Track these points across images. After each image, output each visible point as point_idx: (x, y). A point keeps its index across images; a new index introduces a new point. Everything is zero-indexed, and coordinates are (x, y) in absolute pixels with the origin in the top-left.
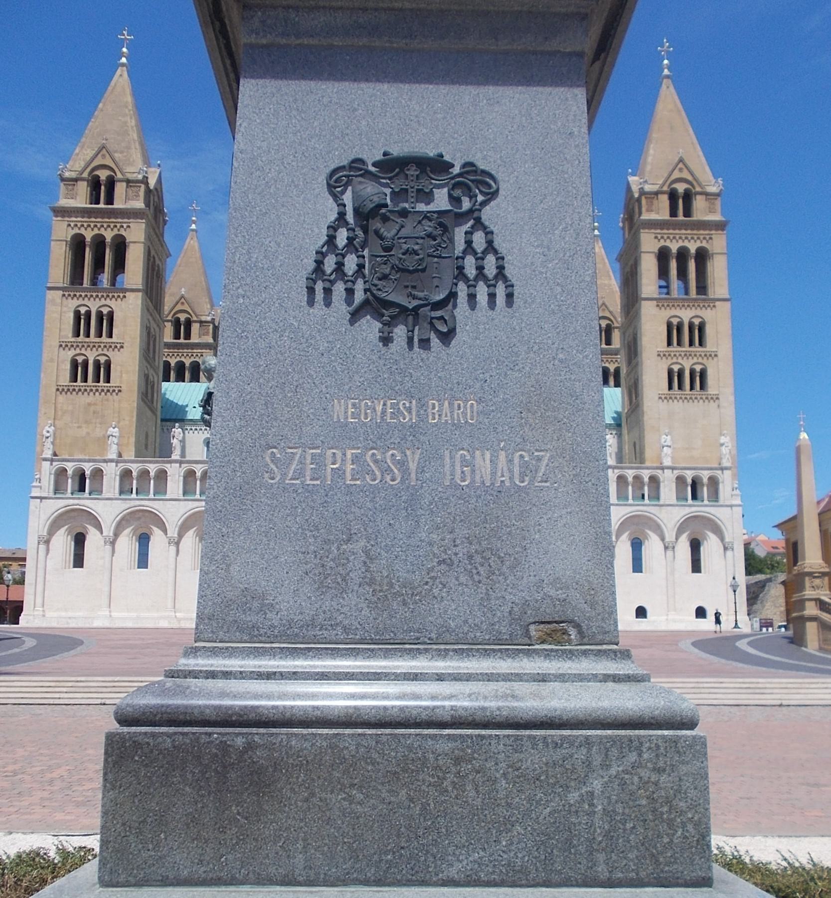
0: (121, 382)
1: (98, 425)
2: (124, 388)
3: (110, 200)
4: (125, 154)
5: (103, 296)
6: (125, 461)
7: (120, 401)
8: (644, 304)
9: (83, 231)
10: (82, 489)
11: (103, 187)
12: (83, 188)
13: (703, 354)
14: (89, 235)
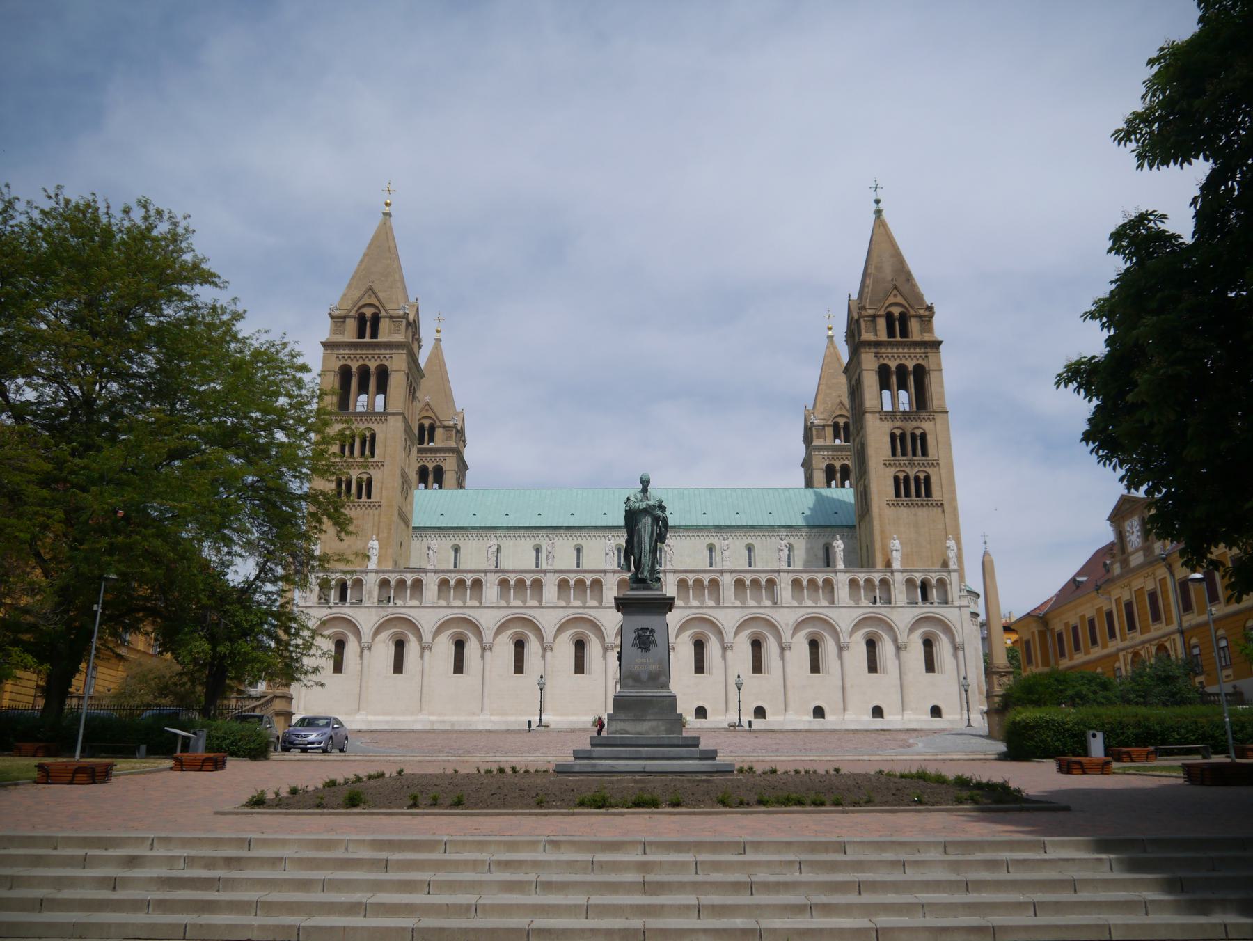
0: (381, 498)
2: (384, 503)
3: (374, 334)
5: (366, 420)
6: (383, 572)
7: (380, 515)
8: (868, 417)
9: (349, 362)
10: (343, 598)
11: (368, 323)
12: (352, 325)
13: (925, 463)
14: (354, 366)
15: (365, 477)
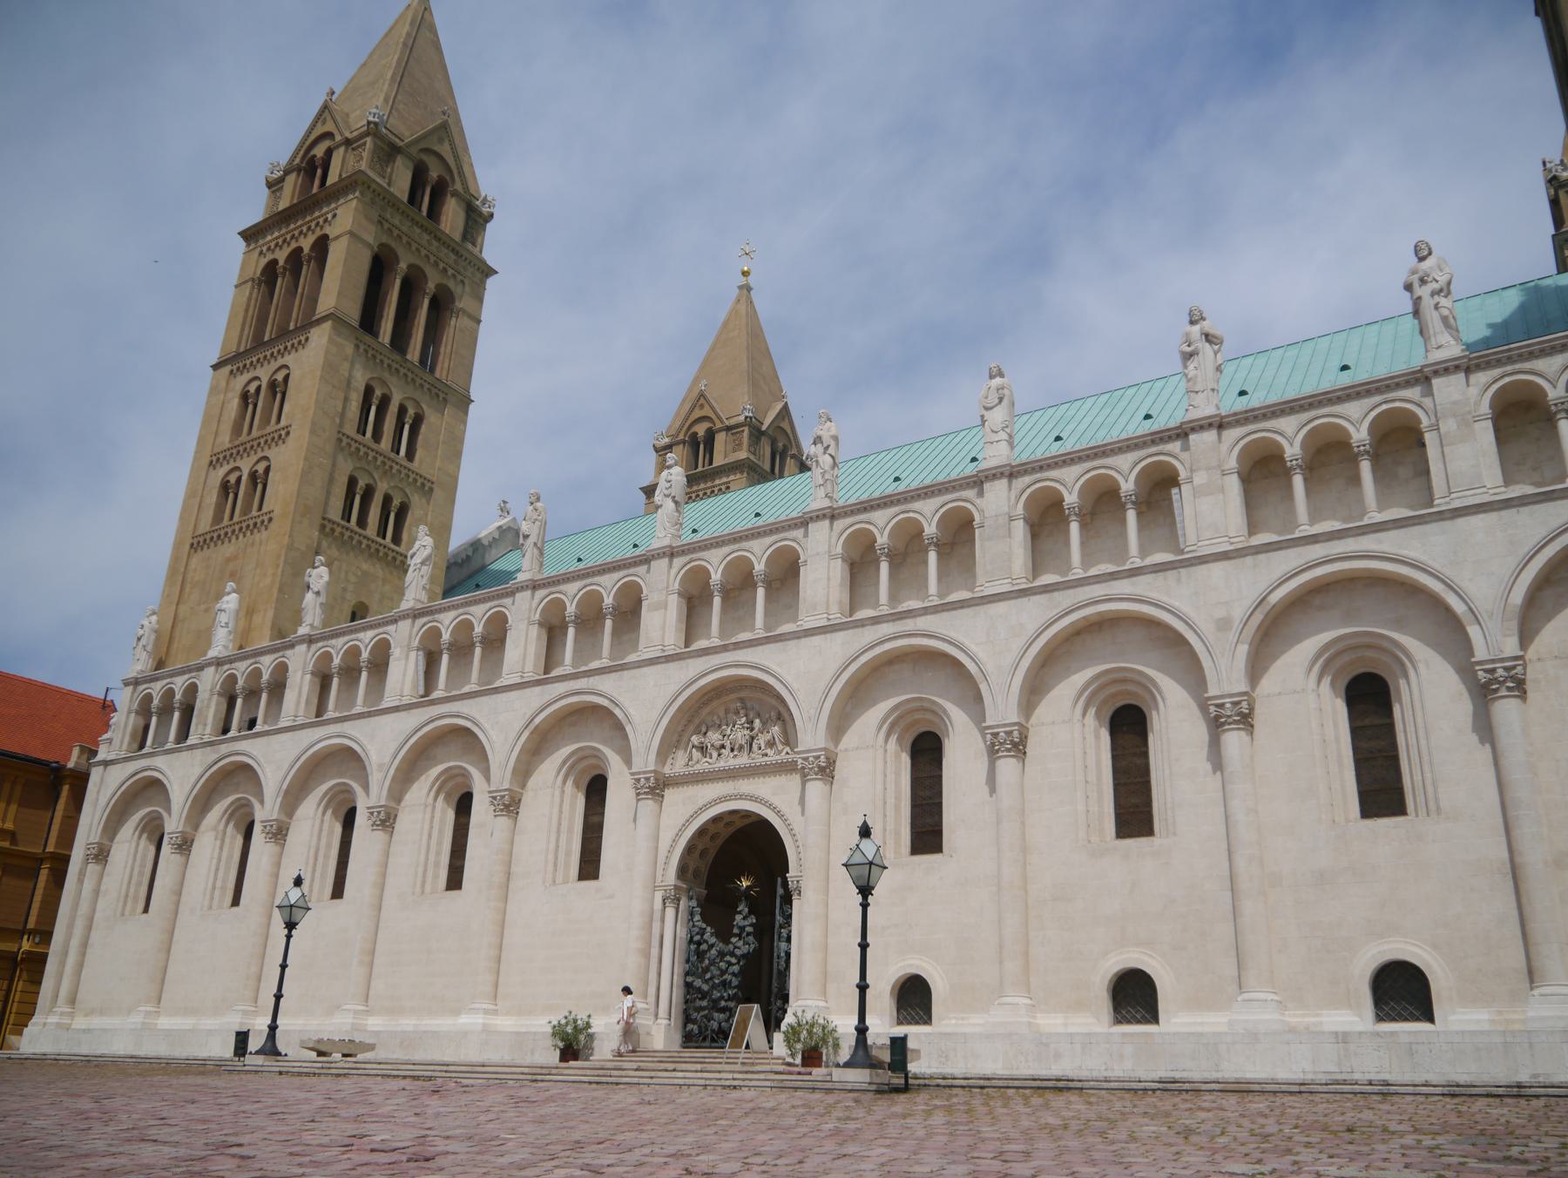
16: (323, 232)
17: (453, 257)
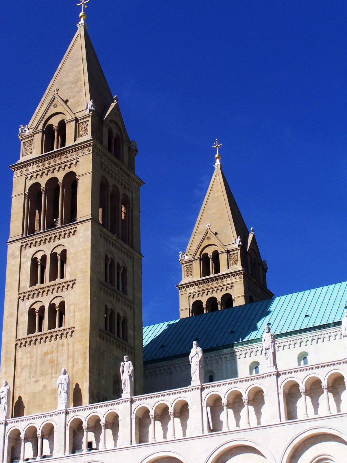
1: (54, 375)
4: (77, 97)
7: (73, 344)
15: (57, 302)
16: (71, 170)
17: (127, 178)
